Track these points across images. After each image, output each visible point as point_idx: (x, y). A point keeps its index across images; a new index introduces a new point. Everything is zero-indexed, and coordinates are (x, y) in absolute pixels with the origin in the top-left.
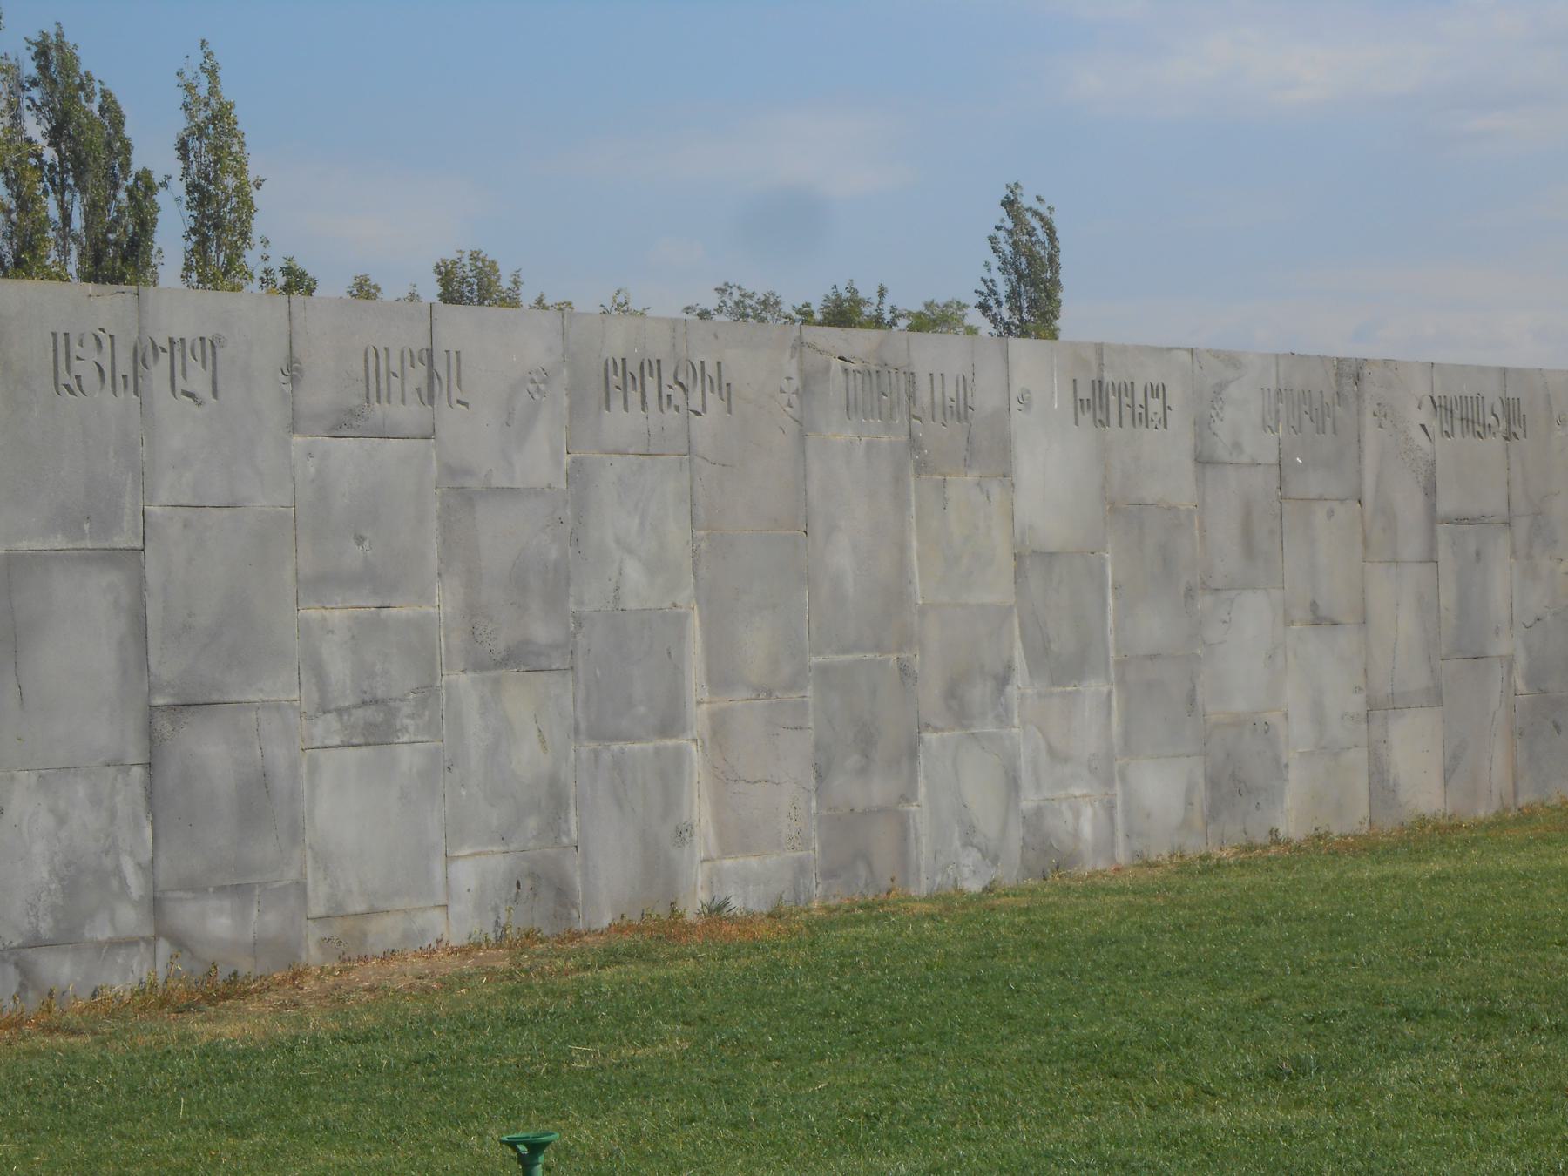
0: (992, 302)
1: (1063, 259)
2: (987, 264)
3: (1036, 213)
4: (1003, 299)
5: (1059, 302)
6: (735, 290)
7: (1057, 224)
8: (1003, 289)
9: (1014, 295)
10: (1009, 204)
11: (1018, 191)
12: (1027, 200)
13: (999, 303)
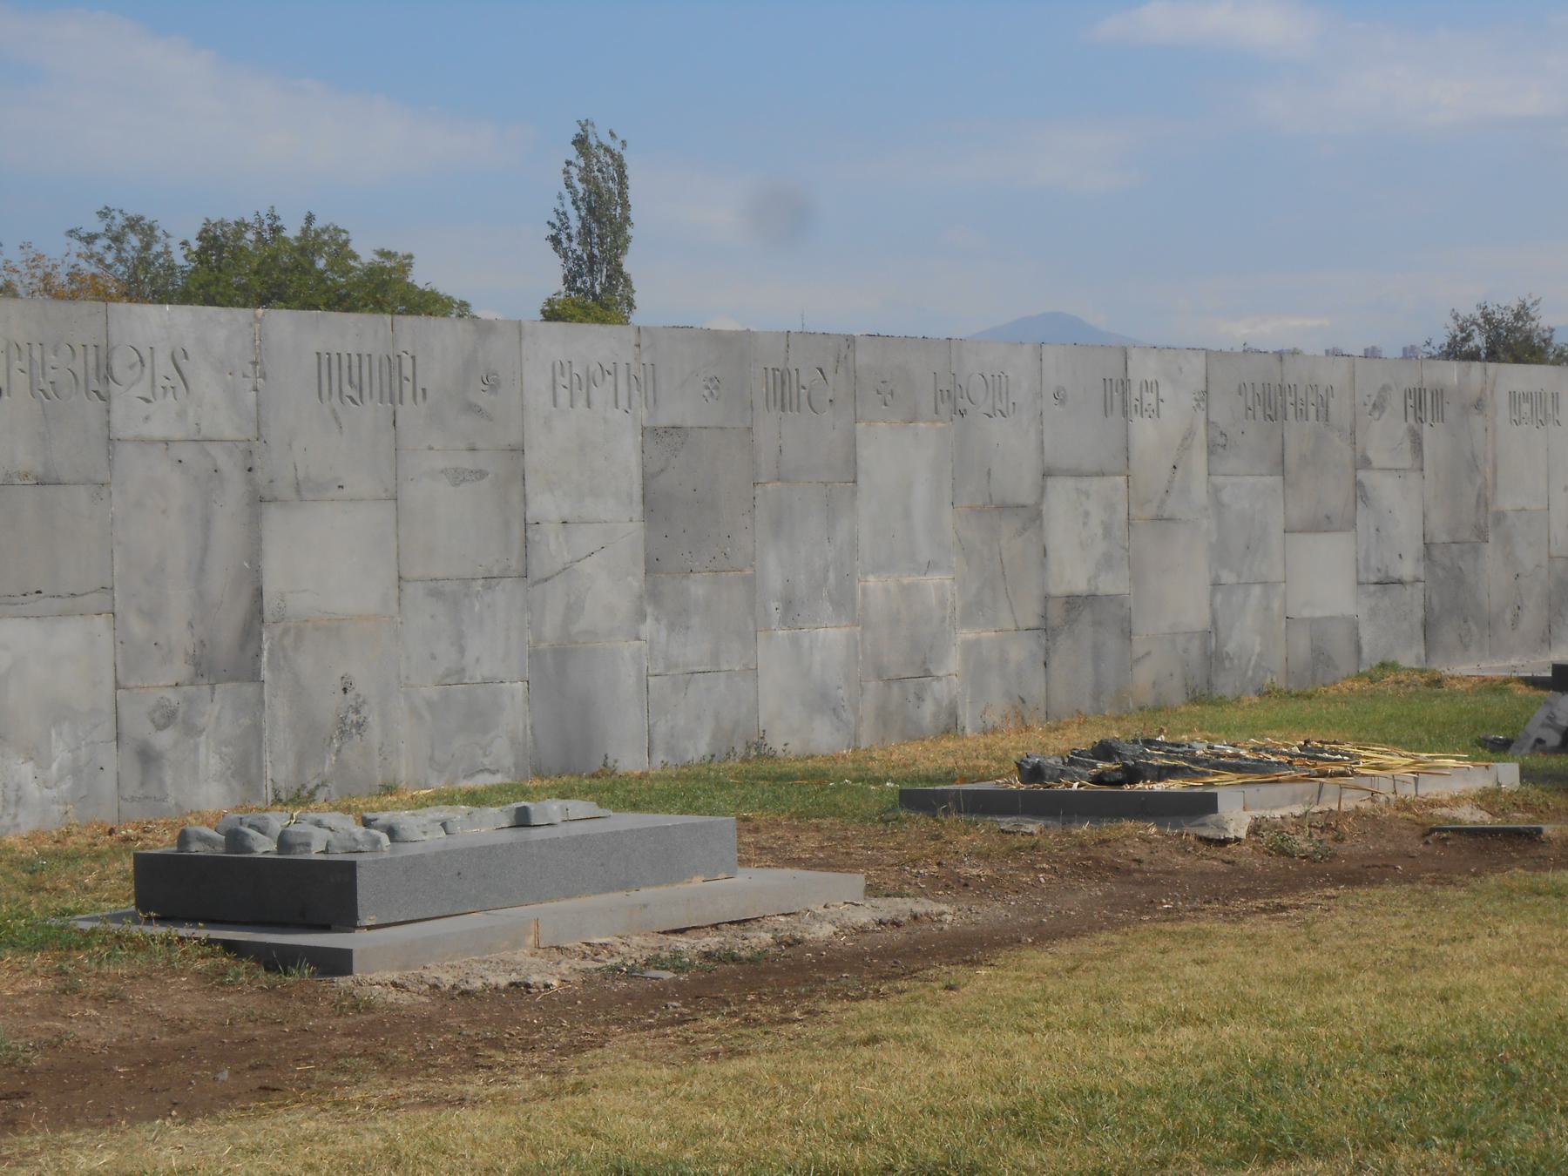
0: (563, 237)
1: (633, 195)
2: (560, 197)
3: (607, 150)
4: (574, 232)
5: (628, 240)
6: (116, 214)
7: (628, 159)
8: (575, 225)
9: (586, 232)
10: (581, 142)
11: (589, 128)
12: (598, 135)
13: (570, 238)
